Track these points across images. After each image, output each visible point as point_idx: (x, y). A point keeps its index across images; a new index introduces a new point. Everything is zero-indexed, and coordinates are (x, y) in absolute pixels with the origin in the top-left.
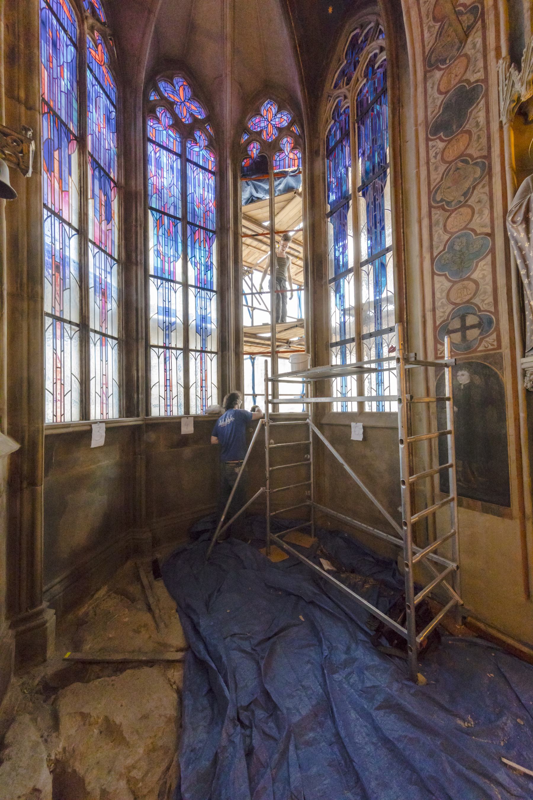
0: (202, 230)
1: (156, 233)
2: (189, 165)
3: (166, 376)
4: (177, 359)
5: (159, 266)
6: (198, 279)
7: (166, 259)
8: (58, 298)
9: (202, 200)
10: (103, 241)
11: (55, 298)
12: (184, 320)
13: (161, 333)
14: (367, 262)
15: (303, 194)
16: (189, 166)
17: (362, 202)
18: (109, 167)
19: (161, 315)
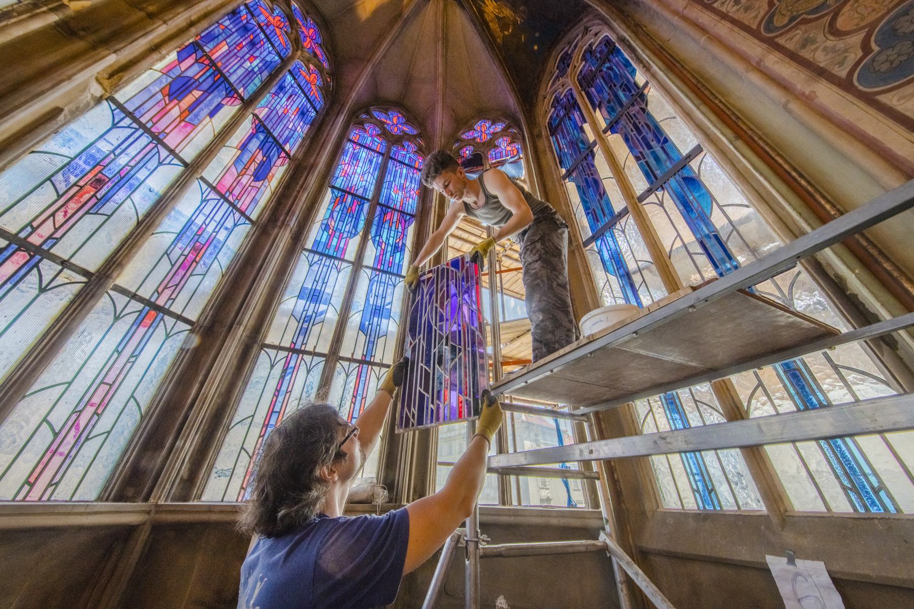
0: (396, 213)
1: (331, 207)
2: (390, 163)
3: (273, 404)
4: (309, 371)
5: (324, 240)
6: (379, 260)
7: (337, 234)
8: (60, 217)
9: (403, 188)
10: (237, 192)
11: (53, 215)
12: (341, 310)
13: (294, 324)
14: (649, 192)
15: (527, 180)
16: (390, 163)
17: (616, 141)
18: (287, 140)
19: (302, 298)
